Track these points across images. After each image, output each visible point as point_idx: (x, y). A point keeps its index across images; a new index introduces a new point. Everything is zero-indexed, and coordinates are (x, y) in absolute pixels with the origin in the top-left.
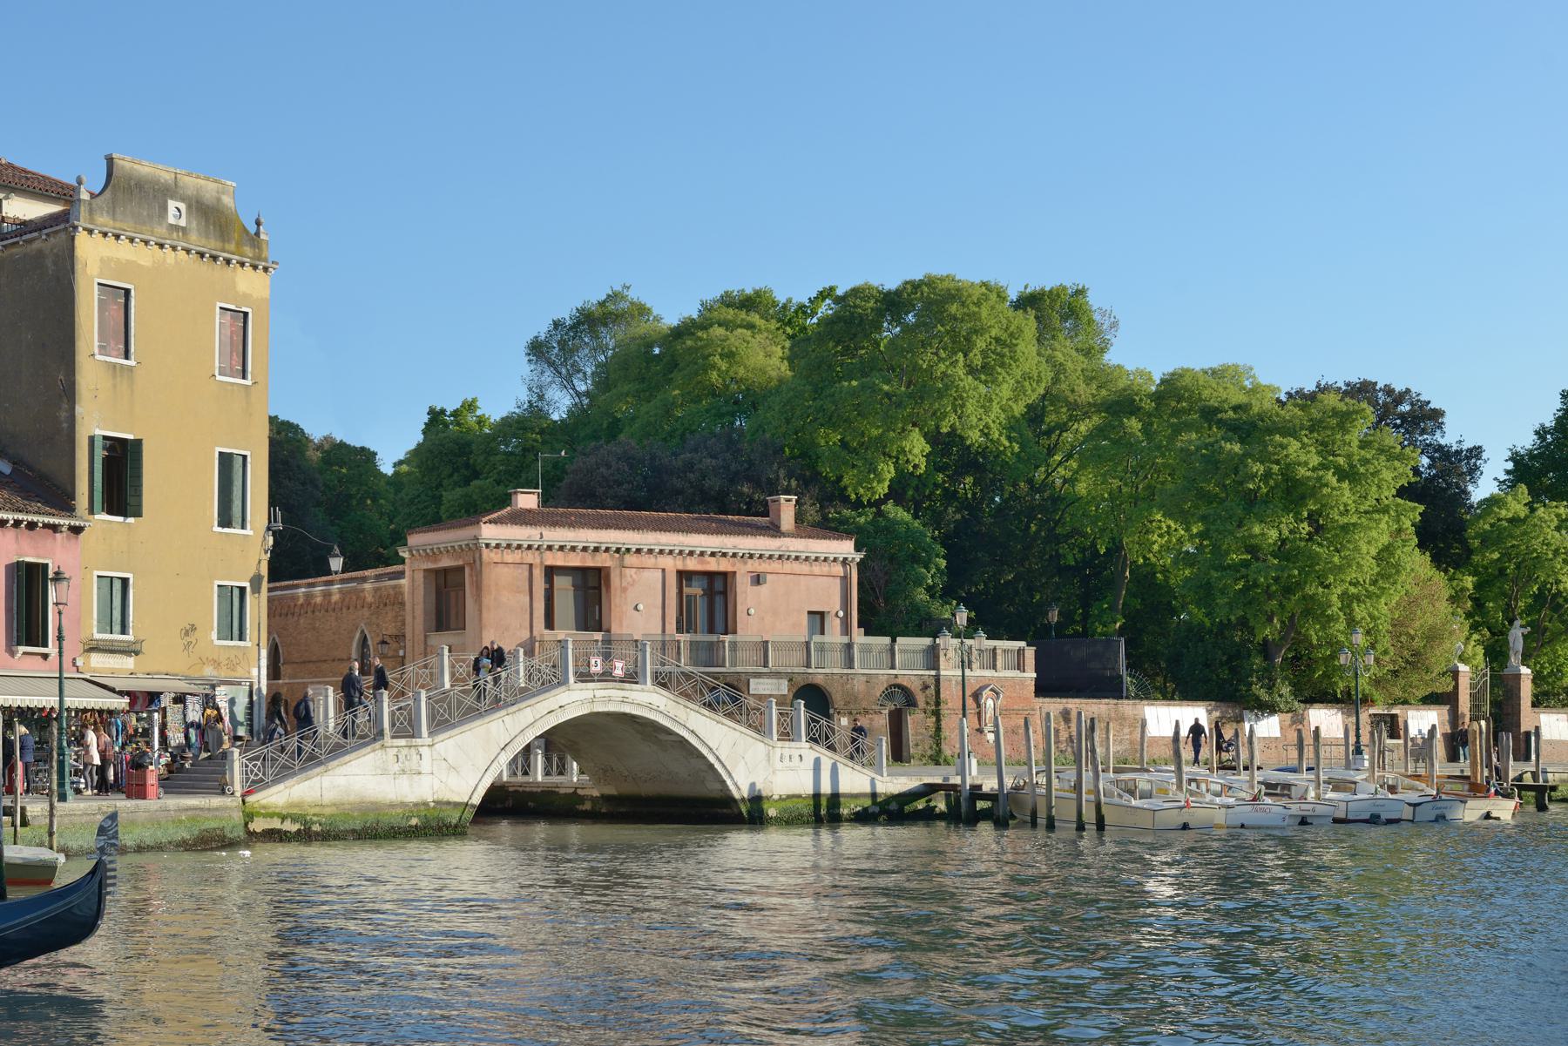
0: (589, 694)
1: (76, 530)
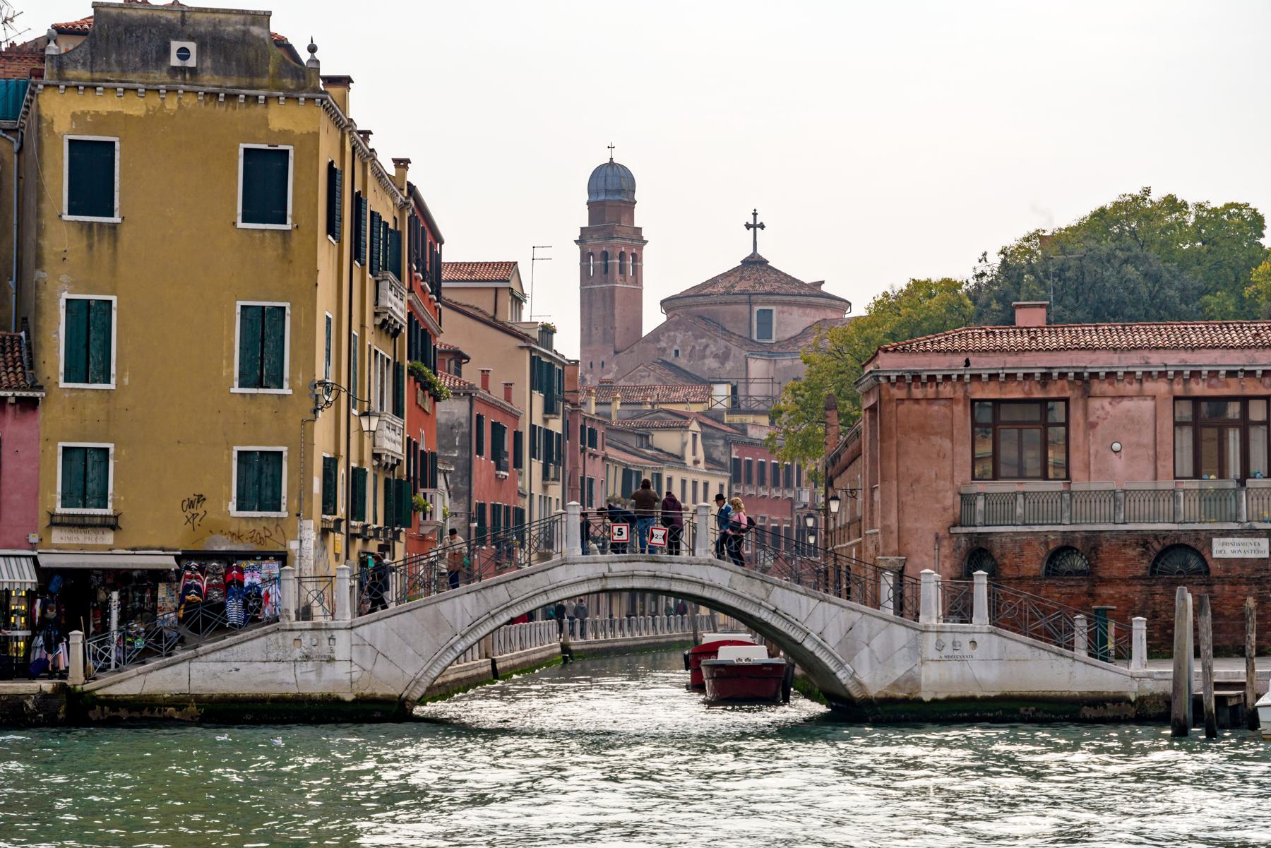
0: (603, 569)
1: (30, 405)
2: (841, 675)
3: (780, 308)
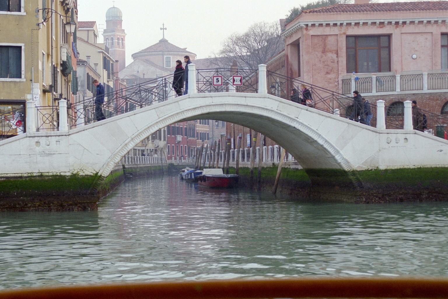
2: (337, 157)
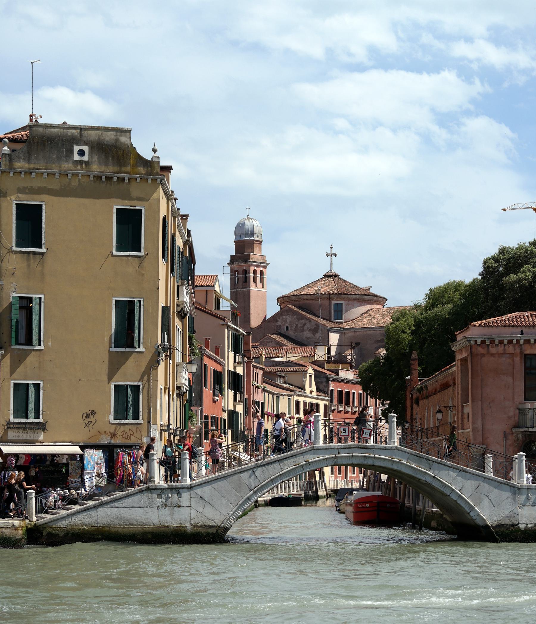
2: (472, 514)
3: (347, 302)
